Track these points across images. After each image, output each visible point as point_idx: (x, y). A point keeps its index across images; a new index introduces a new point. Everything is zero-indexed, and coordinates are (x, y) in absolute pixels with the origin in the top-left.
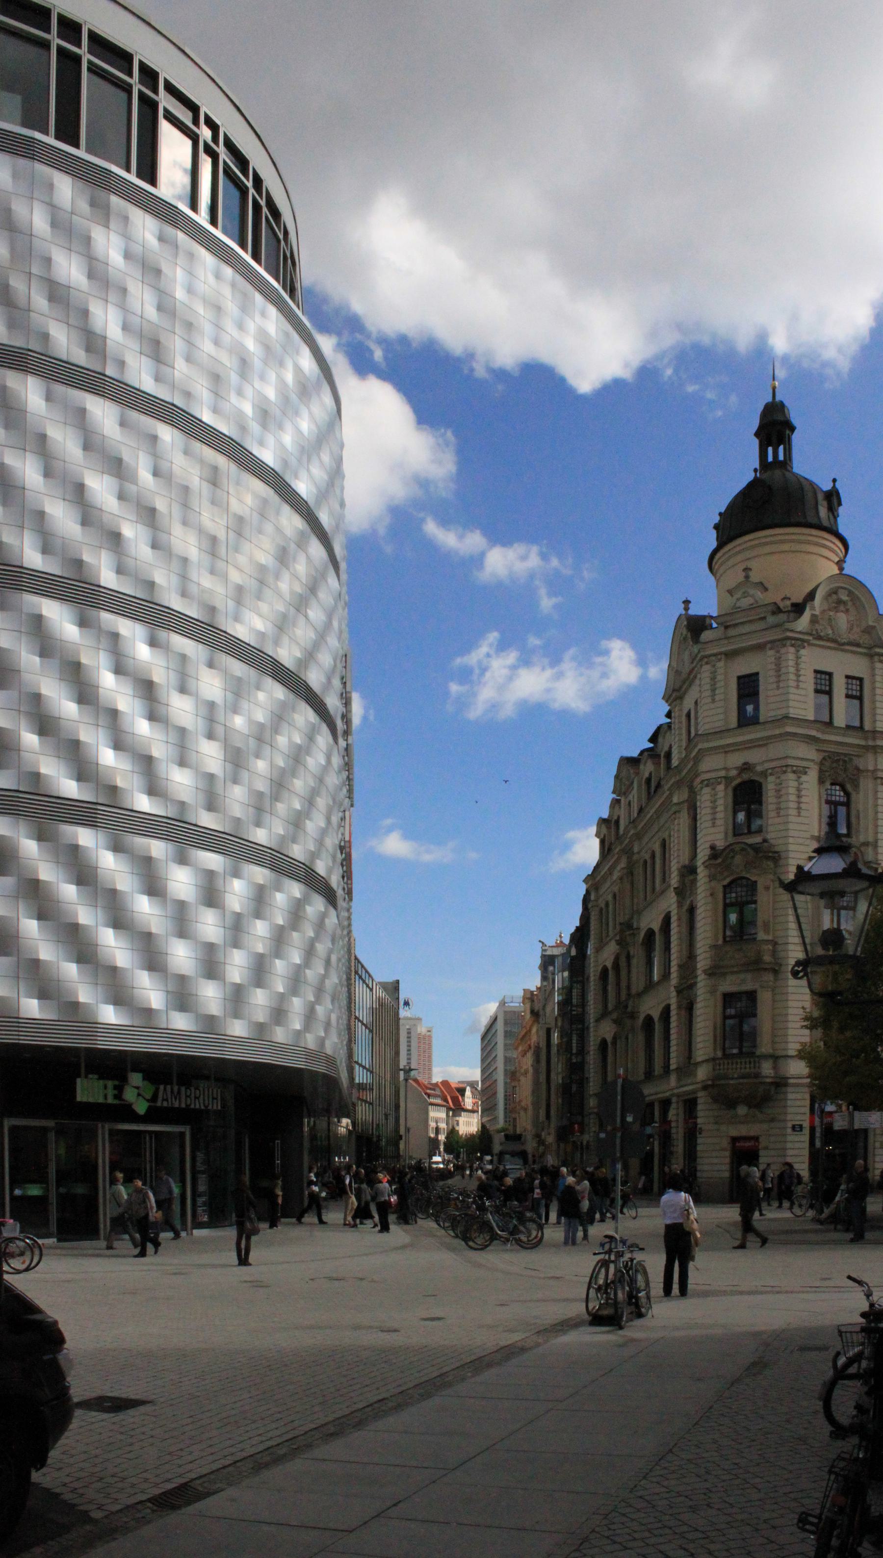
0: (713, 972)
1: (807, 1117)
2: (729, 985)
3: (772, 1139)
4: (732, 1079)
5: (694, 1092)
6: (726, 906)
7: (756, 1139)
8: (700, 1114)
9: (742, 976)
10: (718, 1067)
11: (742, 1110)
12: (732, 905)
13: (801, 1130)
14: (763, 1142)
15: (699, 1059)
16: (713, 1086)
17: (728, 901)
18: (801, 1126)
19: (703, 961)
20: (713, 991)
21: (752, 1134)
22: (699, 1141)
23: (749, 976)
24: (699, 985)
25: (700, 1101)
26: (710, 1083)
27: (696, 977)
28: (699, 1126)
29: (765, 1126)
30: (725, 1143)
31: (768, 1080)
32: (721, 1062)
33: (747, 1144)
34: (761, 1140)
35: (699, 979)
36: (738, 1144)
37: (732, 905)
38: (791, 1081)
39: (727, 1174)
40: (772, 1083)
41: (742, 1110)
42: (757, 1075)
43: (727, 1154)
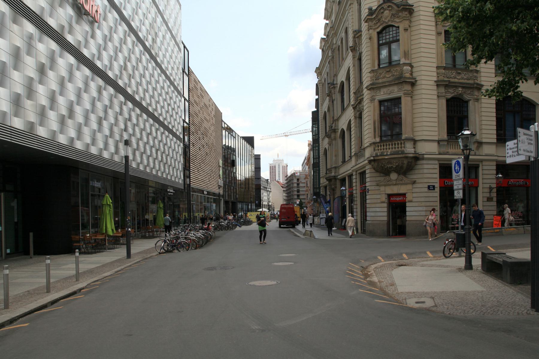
0: (372, 88)
1: (437, 180)
2: (383, 94)
3: (415, 195)
4: (387, 155)
5: (364, 166)
6: (379, 45)
7: (404, 195)
8: (368, 180)
9: (391, 88)
10: (377, 148)
11: (394, 176)
12: (383, 44)
13: (434, 189)
14: (409, 197)
15: (366, 146)
16: (374, 160)
17: (381, 42)
18: (434, 187)
19: (367, 80)
20: (372, 100)
21: (402, 192)
22: (368, 197)
23: (395, 88)
24: (364, 99)
25: (367, 172)
26: (372, 158)
27: (362, 91)
28: (367, 188)
29: (410, 187)
30: (384, 198)
31: (411, 155)
32: (379, 145)
33: (398, 199)
34: (407, 195)
35: (364, 92)
36: (392, 199)
37: (383, 44)
38: (425, 156)
39: (385, 219)
40: (413, 157)
41: (394, 176)
42: (403, 152)
43: (385, 205)
